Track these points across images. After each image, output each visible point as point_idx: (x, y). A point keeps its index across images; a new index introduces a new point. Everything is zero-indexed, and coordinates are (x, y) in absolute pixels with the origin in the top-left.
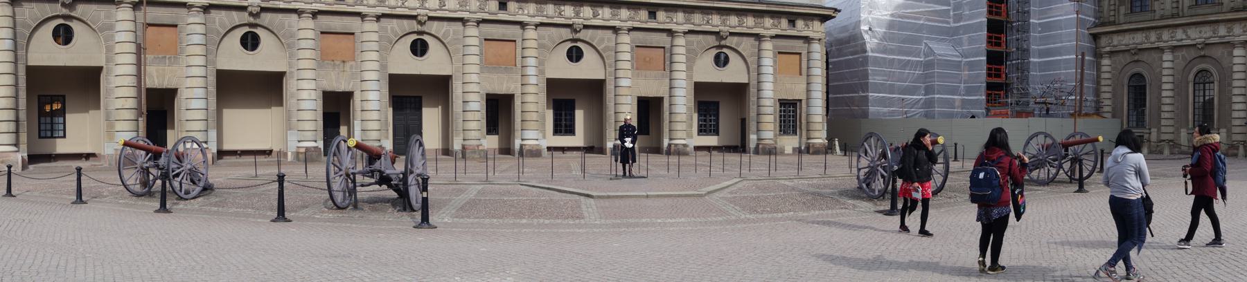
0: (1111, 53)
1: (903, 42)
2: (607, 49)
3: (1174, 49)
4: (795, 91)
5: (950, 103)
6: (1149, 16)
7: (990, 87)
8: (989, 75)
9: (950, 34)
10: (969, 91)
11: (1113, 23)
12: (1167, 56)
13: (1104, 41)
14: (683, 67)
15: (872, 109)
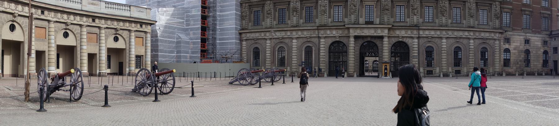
0: (246, 40)
1: (170, 33)
2: (77, 33)
4: (142, 52)
5: (186, 57)
6: (260, 27)
7: (202, 51)
8: (201, 47)
9: (185, 30)
10: (193, 53)
11: (247, 29)
13: (243, 35)
14: (104, 42)
15: (160, 59)
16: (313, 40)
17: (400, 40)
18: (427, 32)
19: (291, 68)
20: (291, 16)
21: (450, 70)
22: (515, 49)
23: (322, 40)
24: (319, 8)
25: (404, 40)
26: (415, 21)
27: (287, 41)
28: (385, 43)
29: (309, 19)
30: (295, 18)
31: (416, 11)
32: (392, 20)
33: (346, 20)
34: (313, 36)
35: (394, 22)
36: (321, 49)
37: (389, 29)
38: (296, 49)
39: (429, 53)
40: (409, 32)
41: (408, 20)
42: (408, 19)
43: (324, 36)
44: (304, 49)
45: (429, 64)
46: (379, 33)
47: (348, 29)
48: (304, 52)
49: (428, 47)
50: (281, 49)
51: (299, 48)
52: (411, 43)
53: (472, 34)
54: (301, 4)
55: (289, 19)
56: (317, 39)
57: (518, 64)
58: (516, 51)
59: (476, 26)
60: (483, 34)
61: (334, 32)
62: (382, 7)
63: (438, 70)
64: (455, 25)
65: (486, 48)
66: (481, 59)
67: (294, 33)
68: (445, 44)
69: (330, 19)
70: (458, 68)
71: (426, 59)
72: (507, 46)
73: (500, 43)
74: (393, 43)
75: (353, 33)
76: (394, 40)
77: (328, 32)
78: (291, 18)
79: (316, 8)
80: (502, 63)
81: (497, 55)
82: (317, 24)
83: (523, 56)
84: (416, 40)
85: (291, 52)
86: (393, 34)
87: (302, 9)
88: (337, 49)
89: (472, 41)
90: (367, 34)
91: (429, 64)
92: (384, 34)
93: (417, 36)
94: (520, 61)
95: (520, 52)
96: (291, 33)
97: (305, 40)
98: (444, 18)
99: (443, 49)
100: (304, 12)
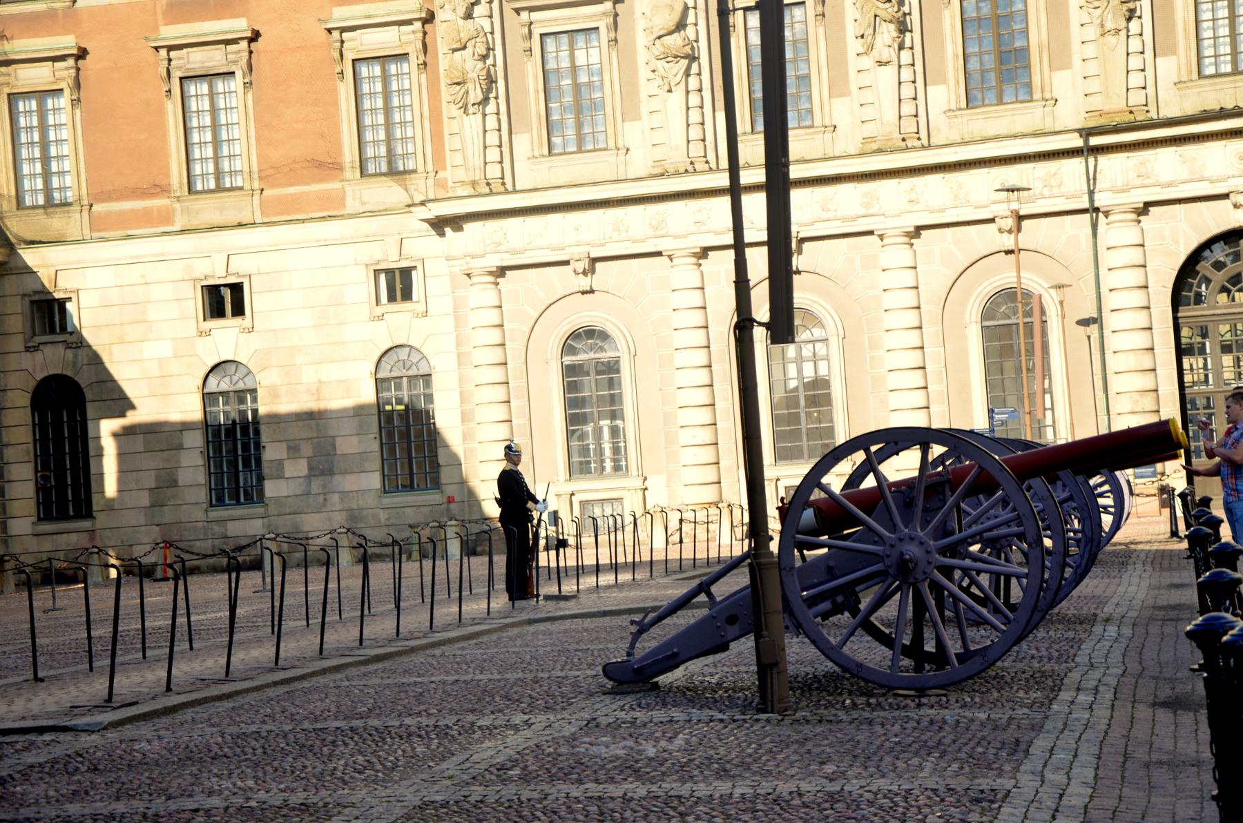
20: (853, 63)
23: (1117, 232)
55: (838, 87)
69: (1169, 68)
78: (854, 81)
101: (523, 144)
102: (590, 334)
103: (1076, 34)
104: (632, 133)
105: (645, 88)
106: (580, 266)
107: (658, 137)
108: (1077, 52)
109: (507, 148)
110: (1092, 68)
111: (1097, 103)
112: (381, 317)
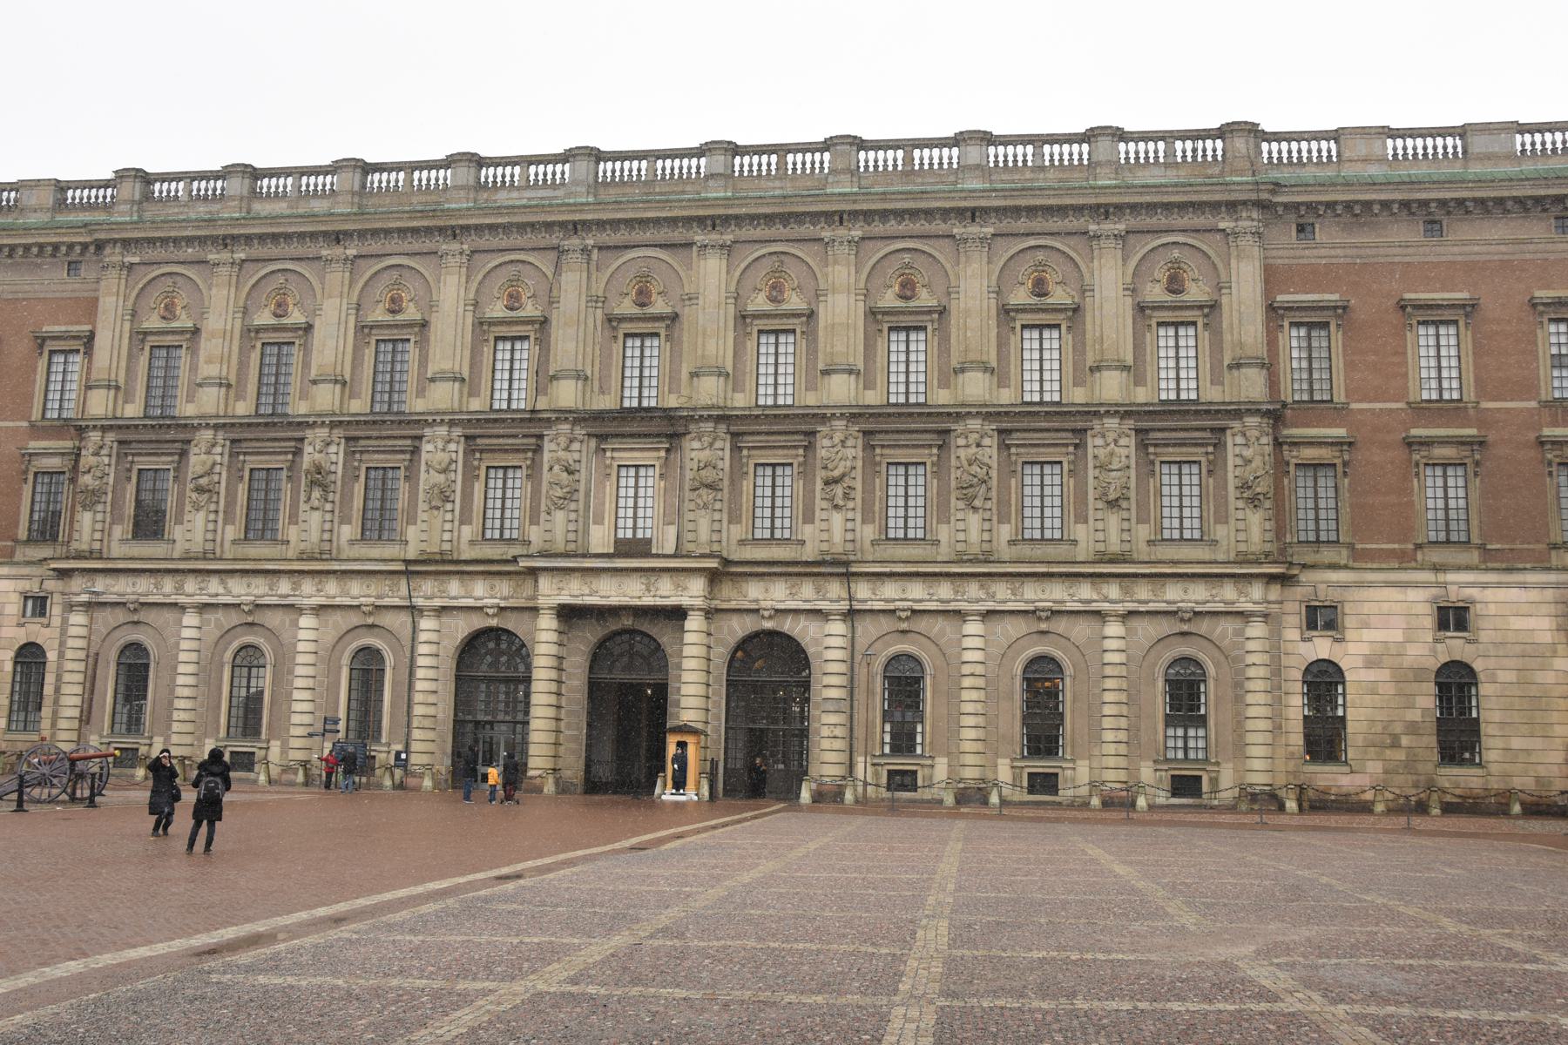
3: (203, 608)
12: (190, 619)
16: (387, 620)
17: (768, 625)
18: (890, 590)
19: (285, 749)
20: (303, 506)
21: (1004, 773)
22: (1371, 662)
24: (423, 476)
25: (787, 626)
26: (838, 536)
27: (273, 619)
28: (688, 638)
29: (378, 524)
30: (316, 517)
31: (839, 490)
32: (737, 531)
33: (535, 534)
34: (387, 601)
35: (742, 542)
36: (421, 661)
37: (714, 577)
38: (310, 659)
39: (904, 687)
40: (807, 590)
41: (808, 531)
42: (808, 528)
43: (437, 603)
44: (346, 660)
45: (903, 742)
46: (665, 593)
47: (533, 572)
48: (345, 672)
49: (896, 658)
50: (248, 658)
51: (327, 658)
52: (817, 642)
53: (1113, 590)
54: (350, 454)
55: (293, 519)
56: (404, 619)
57: (1395, 744)
58: (1385, 675)
59: (1143, 551)
60: (1173, 593)
61: (480, 588)
62: (689, 475)
63: (941, 770)
64: (1026, 551)
65: (1198, 664)
66: (1170, 721)
67: (308, 586)
68: (978, 643)
69: (467, 532)
70: (1041, 766)
71: (886, 716)
72: (1321, 647)
73: (1275, 637)
74: (732, 641)
75: (552, 593)
76: (739, 628)
77: (454, 586)
78: (302, 516)
79: (411, 477)
80: (1297, 740)
81: (1257, 703)
82: (412, 554)
83: (1426, 701)
84: (838, 627)
85: (291, 672)
86: (730, 595)
87: (351, 476)
88: (489, 660)
89: (1114, 629)
90: (614, 601)
91: (903, 742)
92: (685, 601)
93: (844, 605)
94: (1413, 728)
95: (1406, 677)
96: (296, 586)
97: (355, 619)
98: (974, 520)
99: (966, 669)
100: (359, 488)
101: (118, 531)
102: (136, 648)
103: (422, 506)
104: (178, 532)
105: (188, 507)
106: (132, 607)
107: (188, 536)
108: (422, 516)
109: (106, 532)
110: (424, 526)
111: (423, 546)
112: (23, 625)
